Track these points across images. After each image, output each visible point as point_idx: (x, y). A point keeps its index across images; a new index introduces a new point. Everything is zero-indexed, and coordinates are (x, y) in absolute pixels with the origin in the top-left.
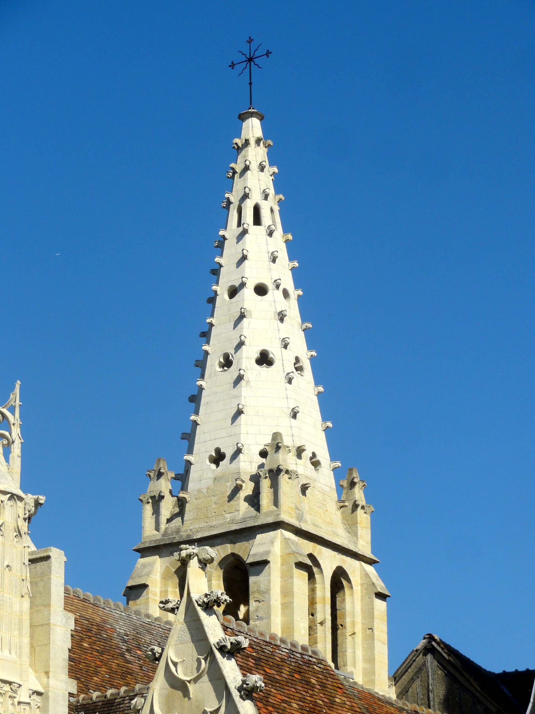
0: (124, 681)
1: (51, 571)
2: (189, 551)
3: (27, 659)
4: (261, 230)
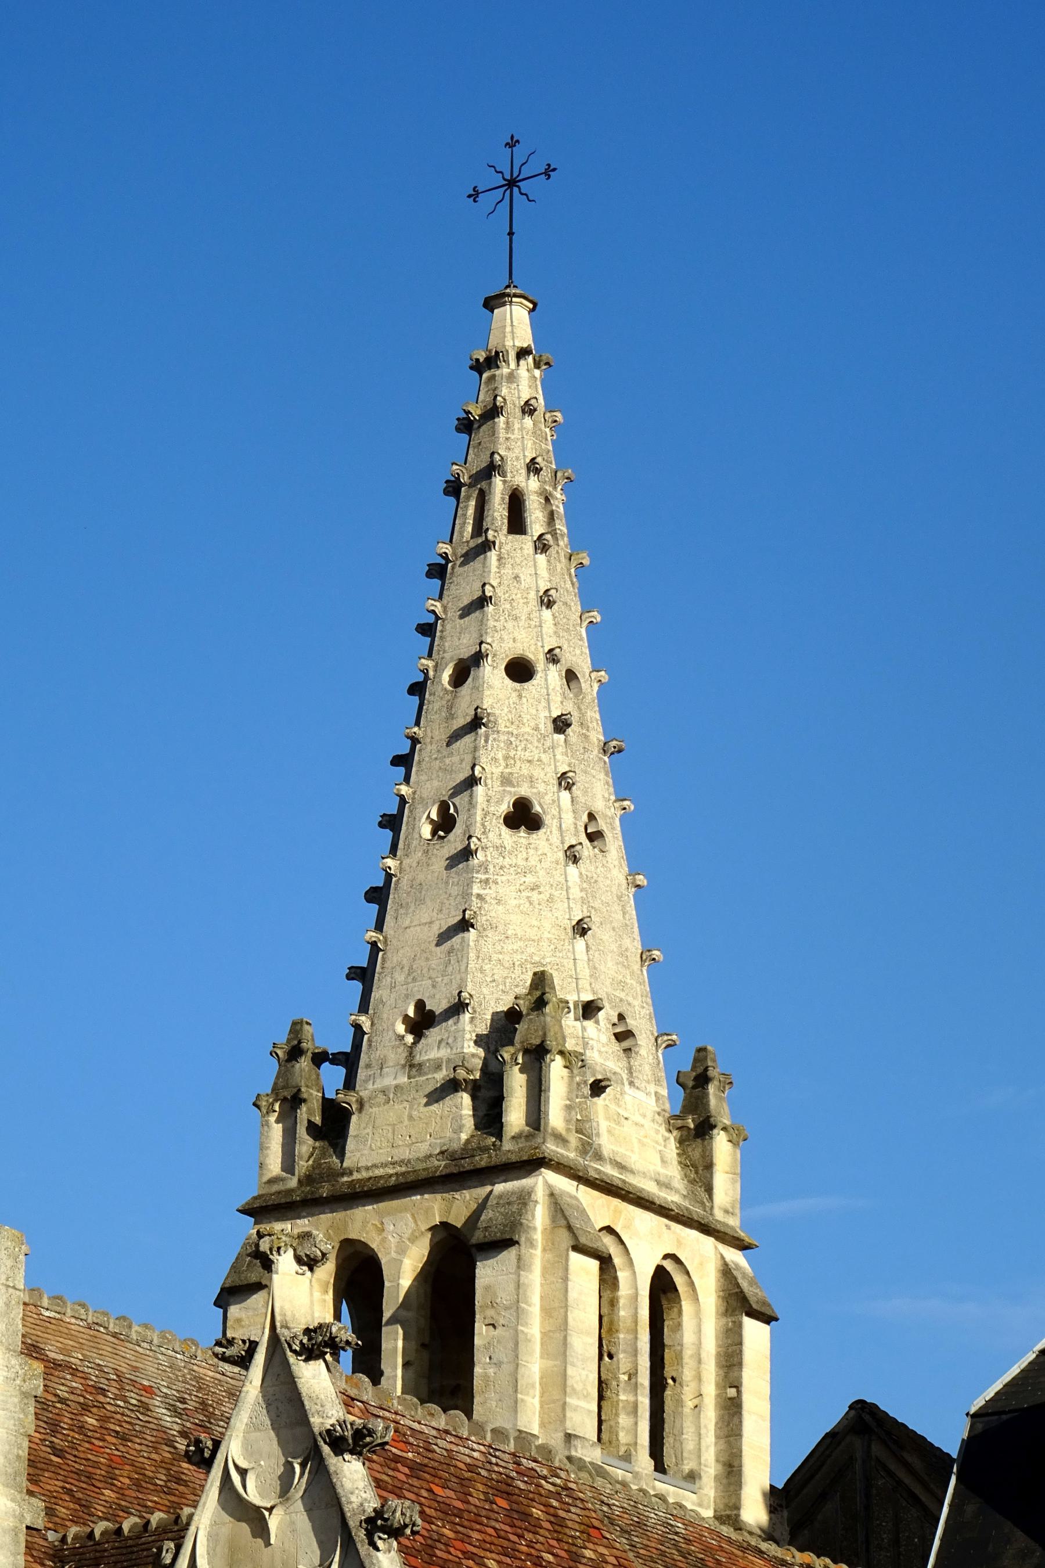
0: (169, 1497)
4: (525, 544)
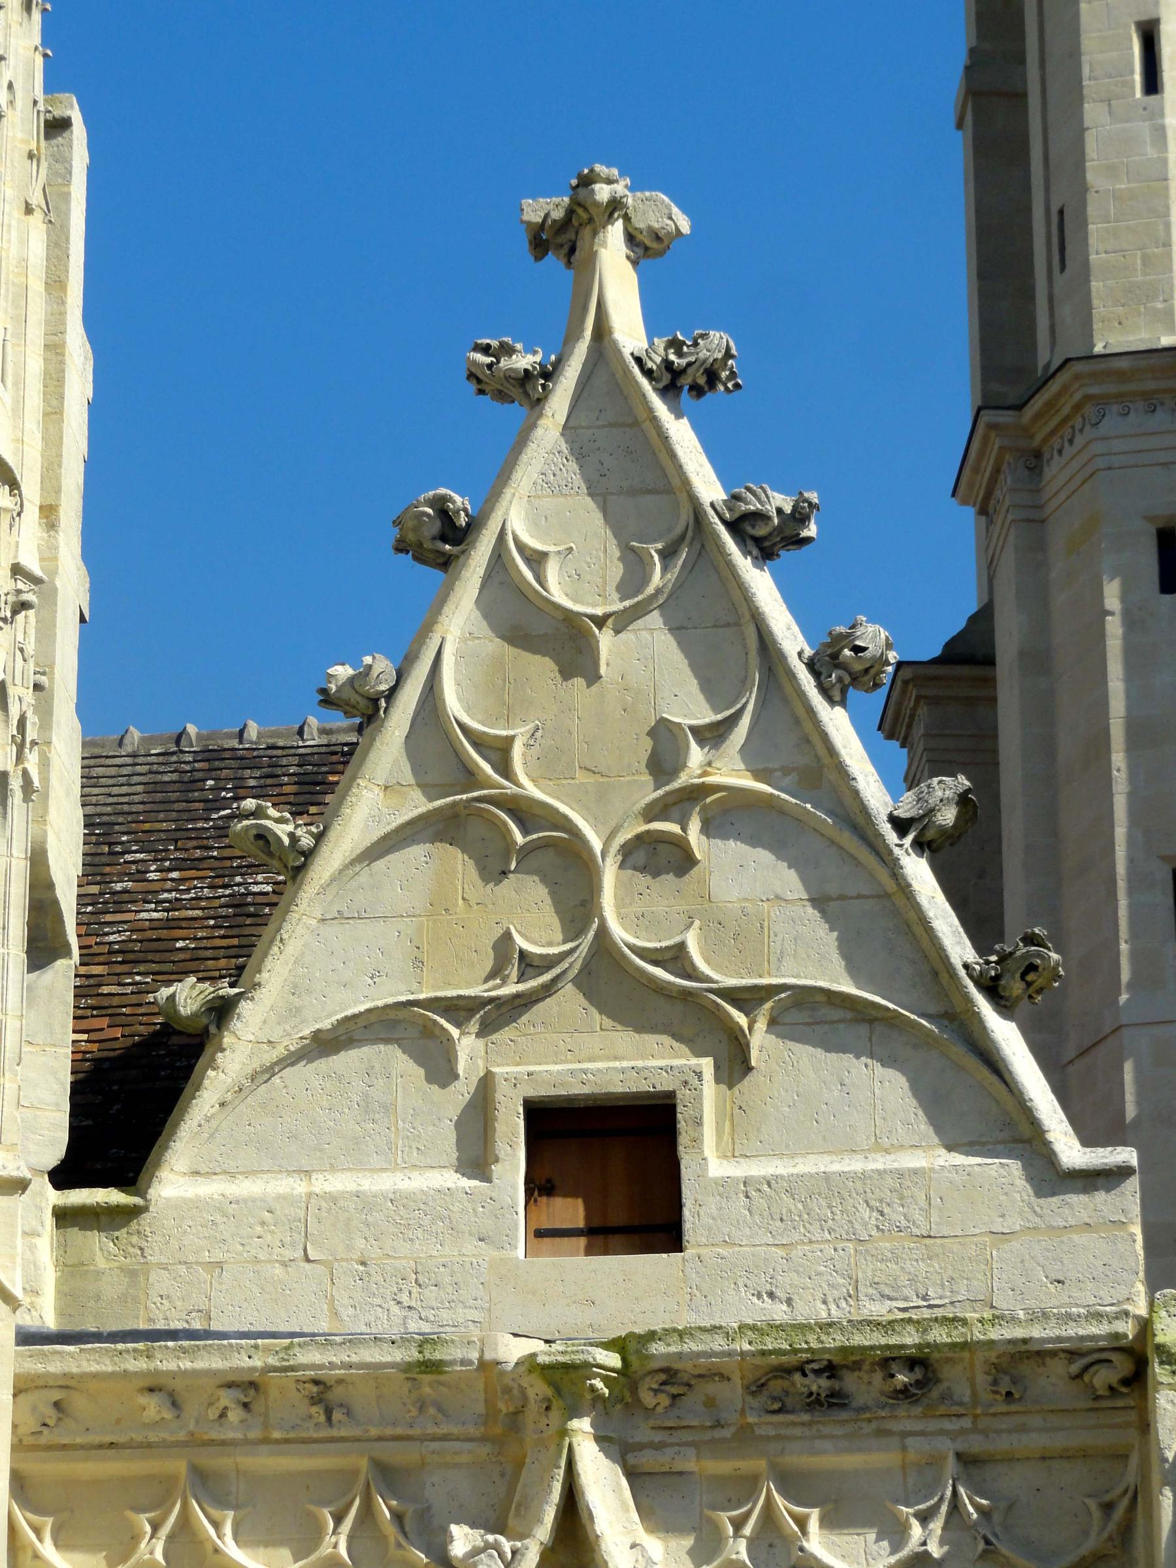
1: (70, 173)
2: (620, 188)
3: (36, 432)
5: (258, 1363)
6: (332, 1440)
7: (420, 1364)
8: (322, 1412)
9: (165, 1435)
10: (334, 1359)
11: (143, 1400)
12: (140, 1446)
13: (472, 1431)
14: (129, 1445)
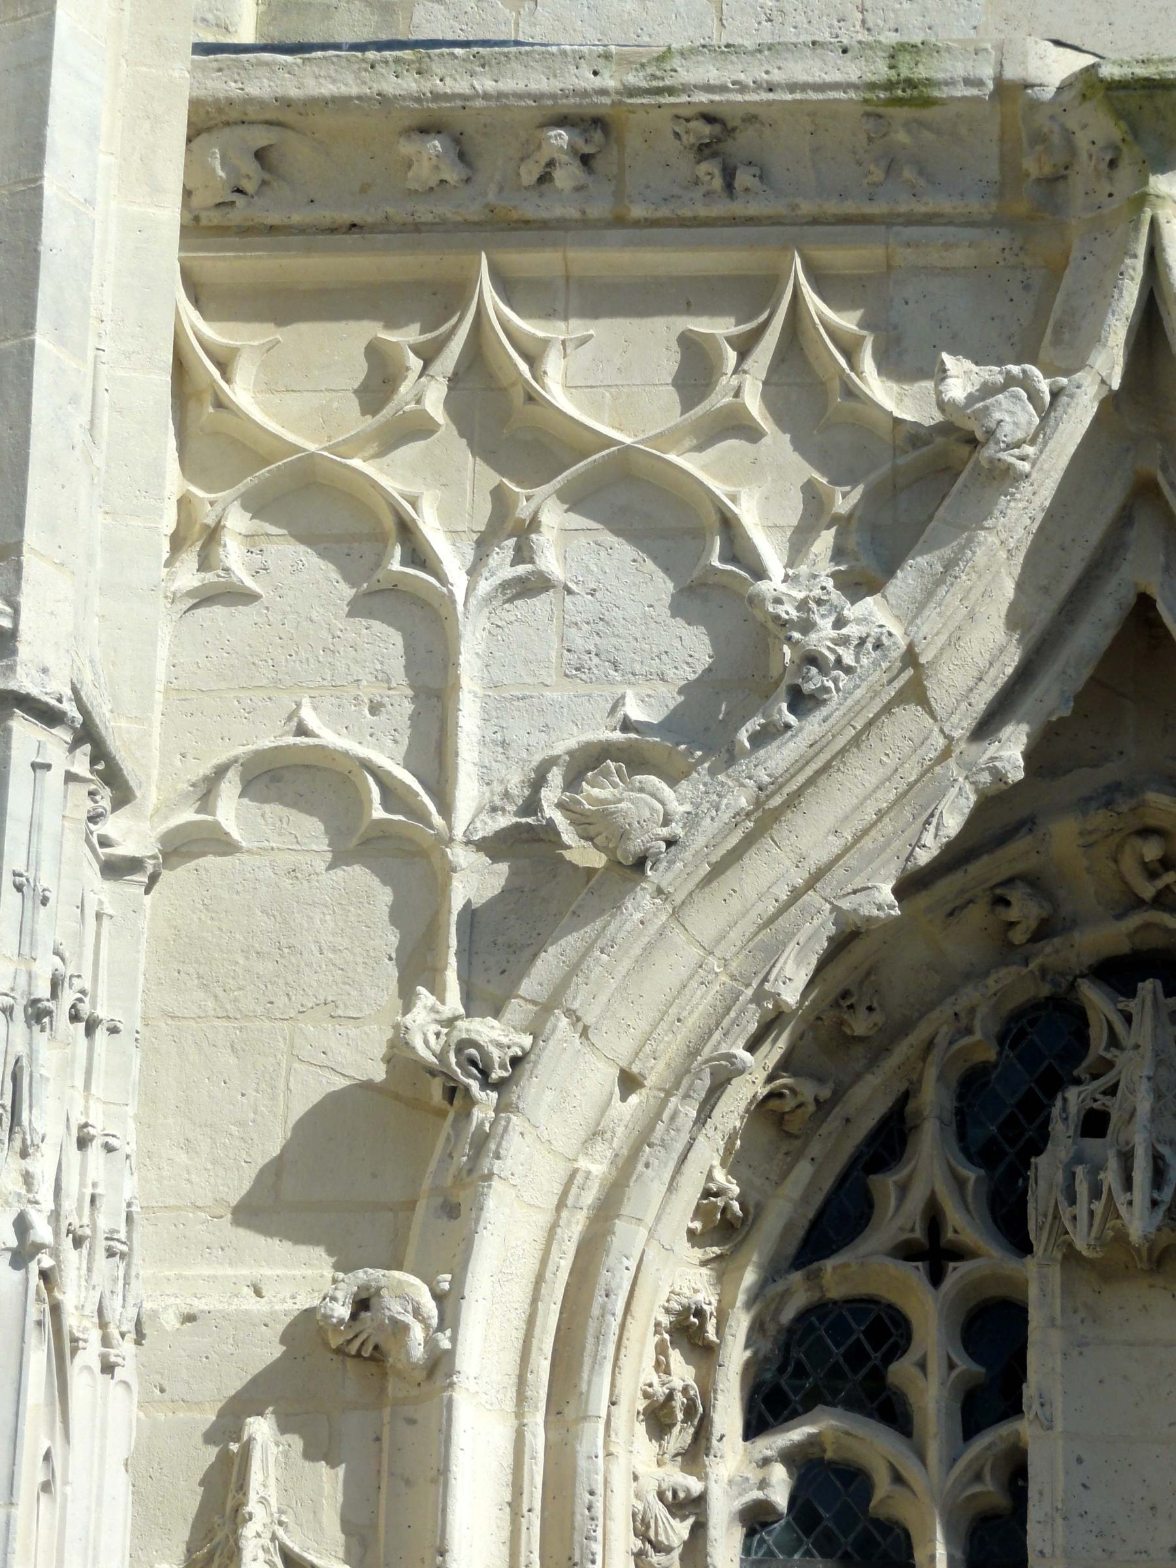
5: (608, 81)
6: (734, 221)
7: (889, 85)
8: (717, 172)
9: (445, 210)
10: (742, 77)
11: (407, 148)
12: (403, 228)
13: (975, 206)
14: (384, 227)
